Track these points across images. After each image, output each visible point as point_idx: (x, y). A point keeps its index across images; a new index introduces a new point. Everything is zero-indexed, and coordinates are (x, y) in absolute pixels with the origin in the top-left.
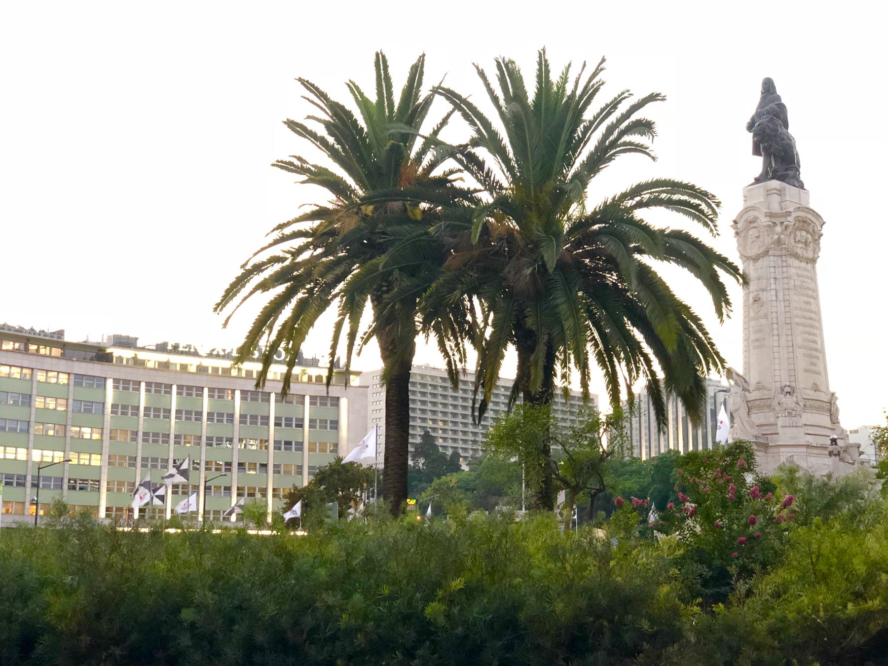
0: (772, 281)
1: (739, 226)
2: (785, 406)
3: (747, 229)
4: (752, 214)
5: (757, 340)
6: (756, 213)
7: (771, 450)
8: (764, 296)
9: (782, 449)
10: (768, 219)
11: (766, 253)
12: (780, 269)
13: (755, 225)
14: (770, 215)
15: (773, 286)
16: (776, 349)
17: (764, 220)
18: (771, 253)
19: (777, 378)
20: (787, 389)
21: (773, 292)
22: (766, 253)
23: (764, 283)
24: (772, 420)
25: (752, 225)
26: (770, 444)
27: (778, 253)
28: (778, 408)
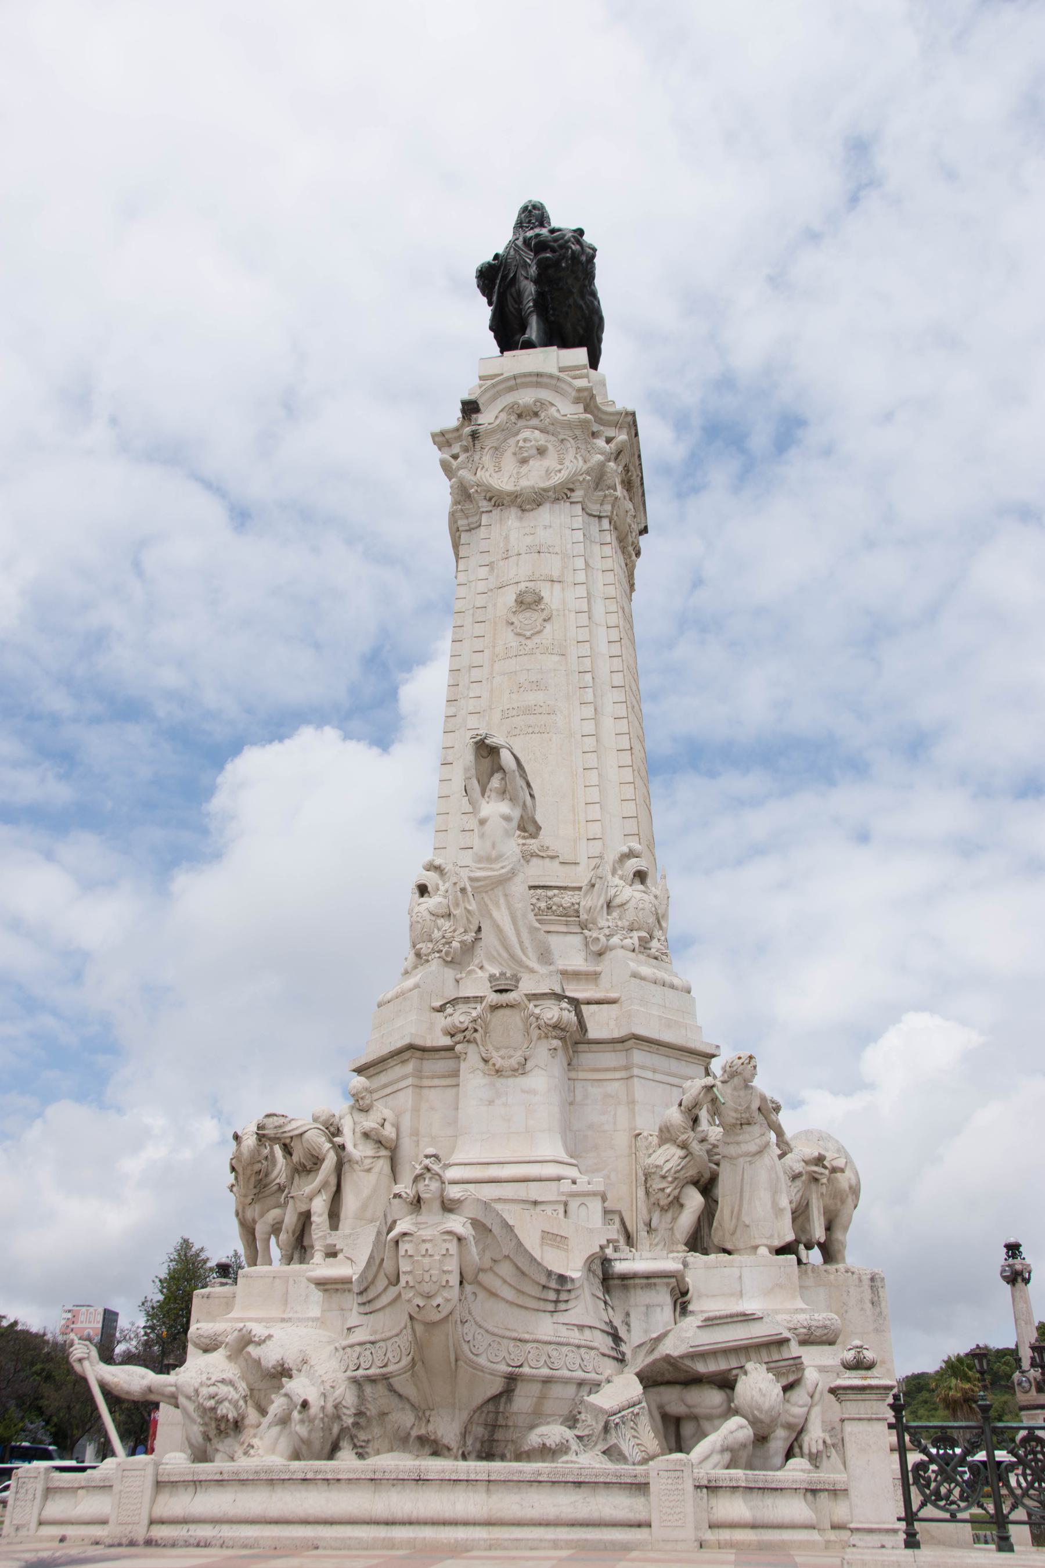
0: (580, 563)
1: (486, 419)
2: (630, 915)
3: (507, 431)
4: (526, 397)
5: (529, 711)
6: (544, 394)
7: (589, 1058)
8: (553, 597)
9: (639, 1056)
10: (580, 408)
11: (563, 493)
12: (597, 548)
13: (535, 422)
15: (581, 577)
16: (590, 743)
17: (566, 409)
18: (578, 495)
19: (595, 829)
20: (633, 865)
21: (581, 591)
22: (563, 493)
23: (553, 566)
24: (577, 961)
25: (521, 423)
26: (593, 1034)
27: (594, 508)
28: (604, 921)
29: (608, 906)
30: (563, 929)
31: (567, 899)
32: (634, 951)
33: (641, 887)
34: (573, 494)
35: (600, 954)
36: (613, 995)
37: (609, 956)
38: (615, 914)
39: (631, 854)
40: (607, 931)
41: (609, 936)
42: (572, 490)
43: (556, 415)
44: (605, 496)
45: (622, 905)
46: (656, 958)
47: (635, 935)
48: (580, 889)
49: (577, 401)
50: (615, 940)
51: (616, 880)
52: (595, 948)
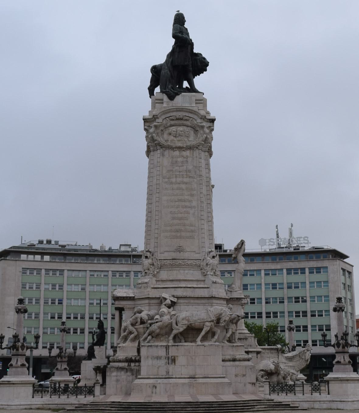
9: (215, 301)
14: (204, 118)
29: (207, 264)
30: (196, 269)
31: (198, 262)
32: (212, 275)
33: (214, 260)
34: (199, 147)
35: (205, 275)
36: (209, 286)
37: (207, 276)
38: (208, 267)
39: (211, 251)
40: (206, 271)
41: (207, 272)
42: (199, 146)
43: (196, 123)
44: (207, 146)
45: (210, 264)
46: (216, 276)
47: (213, 271)
48: (201, 260)
49: (201, 118)
50: (208, 273)
51: (208, 258)
52: (205, 274)
